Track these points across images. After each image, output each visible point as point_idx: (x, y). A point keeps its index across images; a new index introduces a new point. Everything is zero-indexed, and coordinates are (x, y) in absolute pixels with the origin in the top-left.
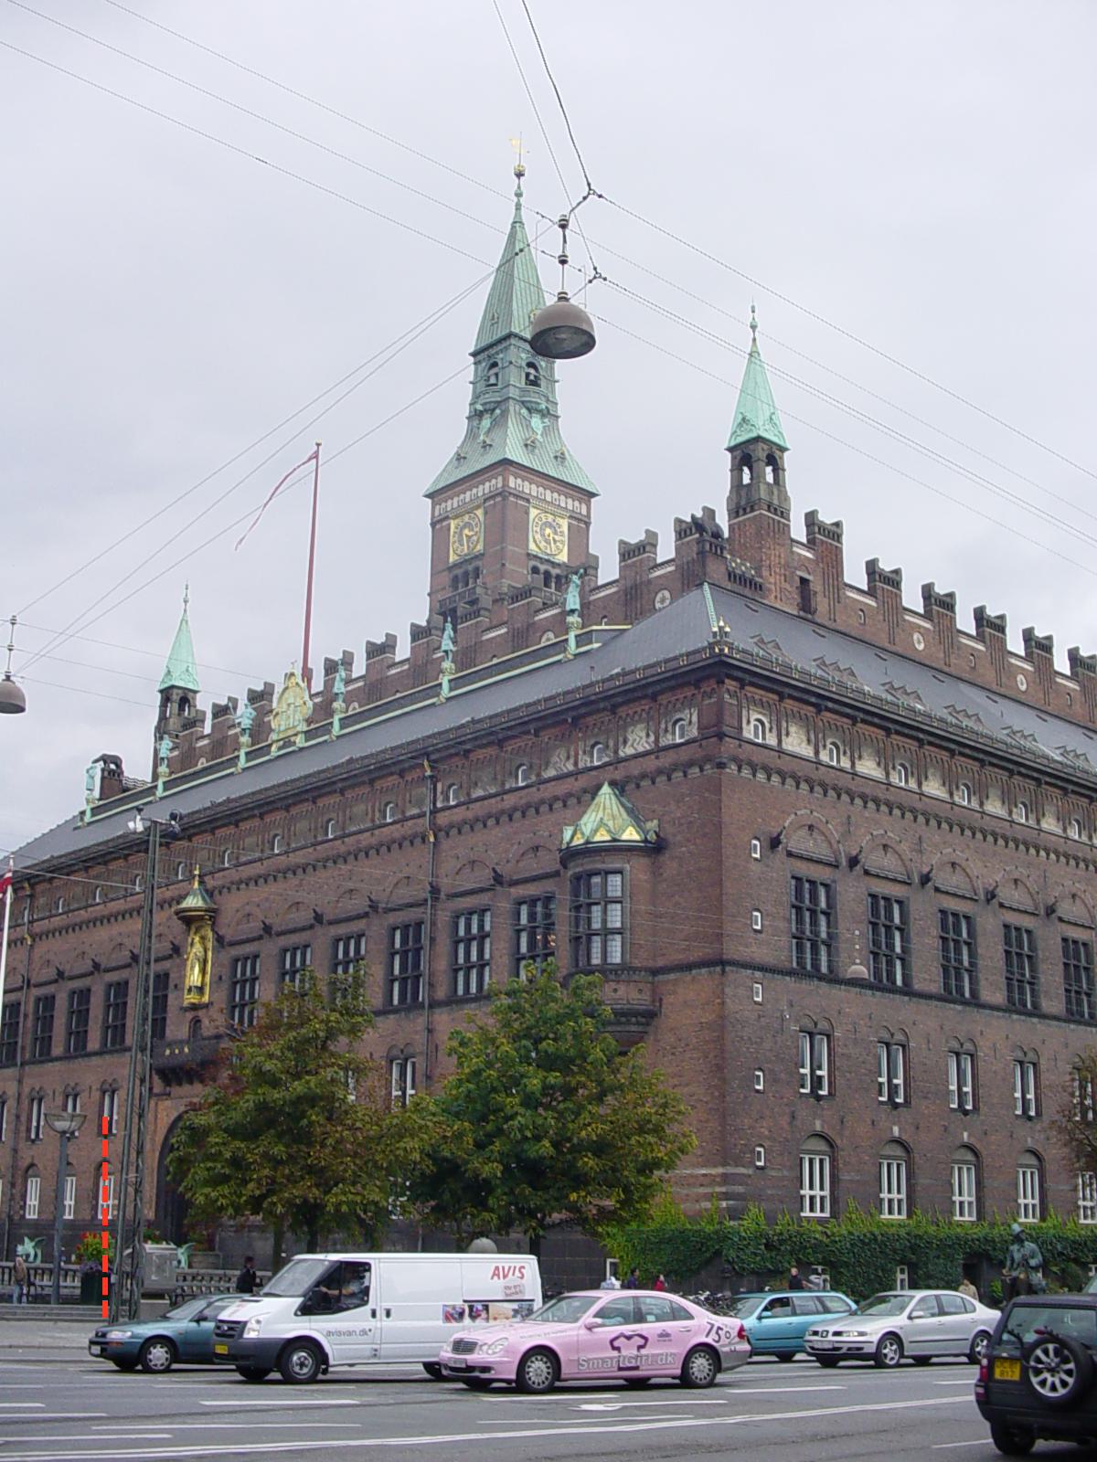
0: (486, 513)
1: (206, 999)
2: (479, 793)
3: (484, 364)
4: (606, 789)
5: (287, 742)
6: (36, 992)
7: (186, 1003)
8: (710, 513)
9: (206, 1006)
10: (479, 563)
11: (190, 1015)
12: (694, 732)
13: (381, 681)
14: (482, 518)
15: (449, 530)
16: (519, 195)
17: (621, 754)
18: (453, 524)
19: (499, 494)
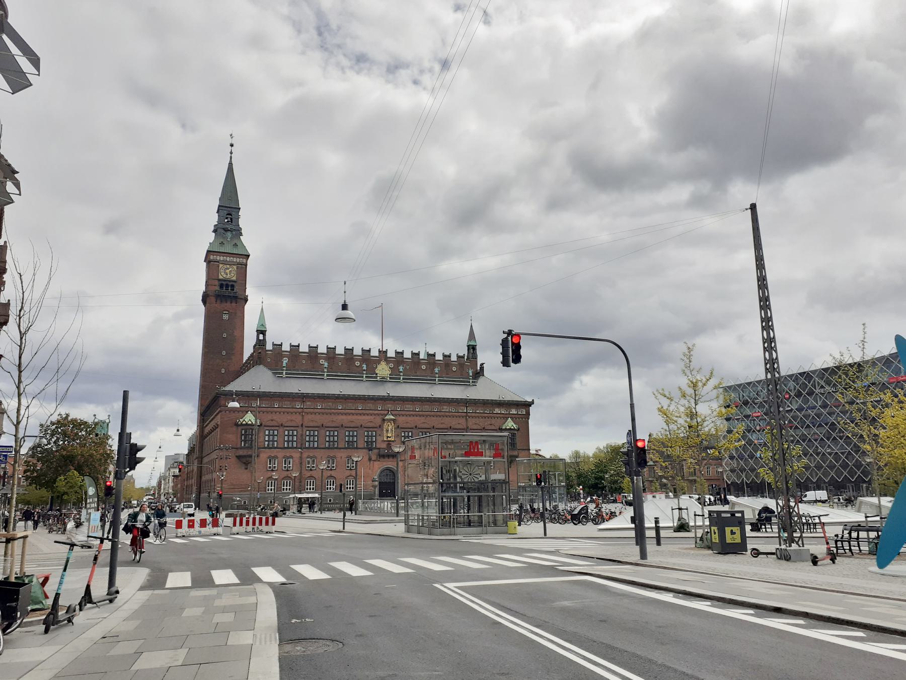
0: (237, 268)
1: (393, 439)
2: (478, 411)
3: (225, 212)
4: (509, 419)
5: (383, 378)
6: (305, 429)
7: (385, 439)
8: (464, 355)
9: (393, 441)
10: (233, 283)
11: (387, 443)
12: (525, 413)
13: (368, 359)
14: (236, 269)
15: (219, 266)
16: (231, 153)
17: (511, 413)
18: (221, 266)
19: (245, 265)
